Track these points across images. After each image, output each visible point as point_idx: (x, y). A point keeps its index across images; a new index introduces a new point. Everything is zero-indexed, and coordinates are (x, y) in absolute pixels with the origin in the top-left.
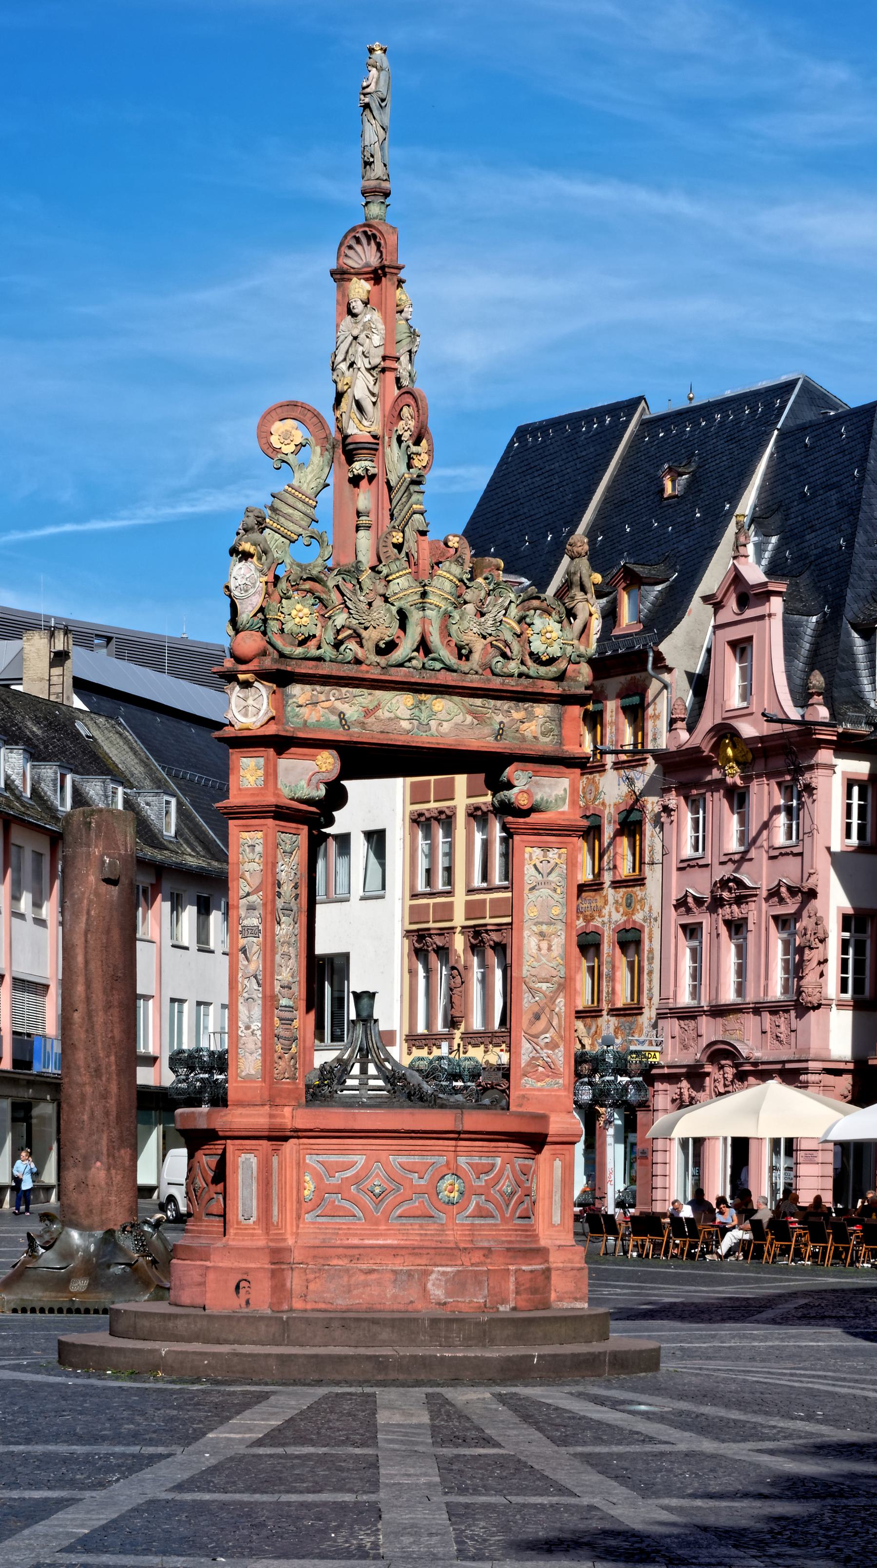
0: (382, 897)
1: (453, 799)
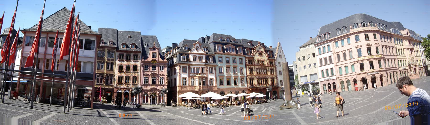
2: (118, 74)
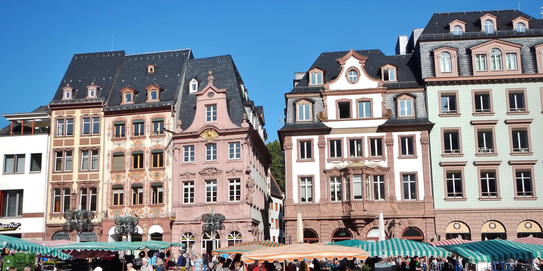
0: (40, 173)
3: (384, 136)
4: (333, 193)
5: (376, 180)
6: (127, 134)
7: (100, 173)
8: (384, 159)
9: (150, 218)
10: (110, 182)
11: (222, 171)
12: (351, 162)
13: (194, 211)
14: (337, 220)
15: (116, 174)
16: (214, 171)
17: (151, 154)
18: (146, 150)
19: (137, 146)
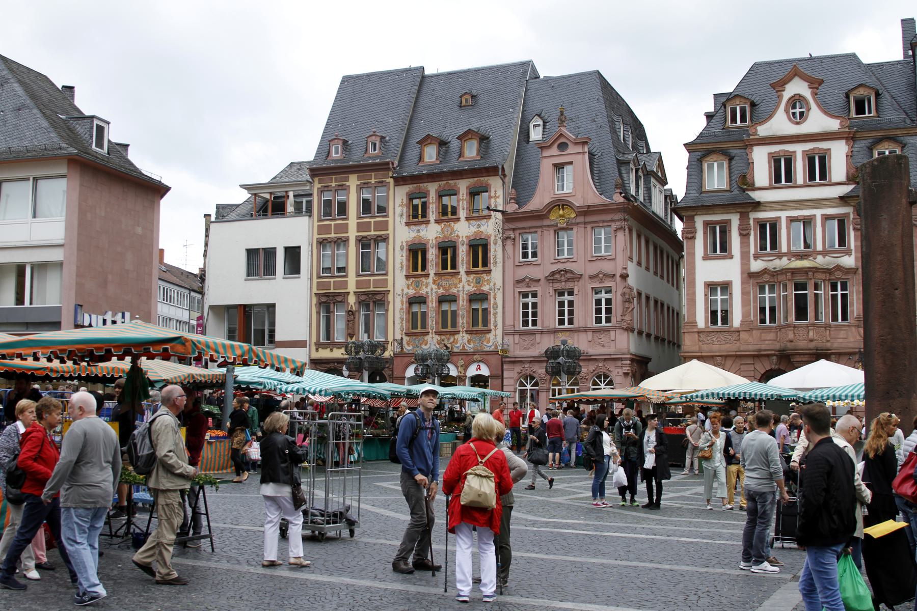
0: (299, 278)
1: (347, 233)
2: (406, 291)
3: (848, 214)
4: (763, 310)
5: (834, 288)
6: (431, 214)
7: (390, 277)
8: (848, 253)
9: (469, 350)
10: (405, 292)
11: (581, 275)
12: (793, 259)
13: (538, 341)
14: (768, 356)
15: (414, 279)
16: (569, 275)
17: (468, 247)
18: (461, 239)
19: (446, 233)
